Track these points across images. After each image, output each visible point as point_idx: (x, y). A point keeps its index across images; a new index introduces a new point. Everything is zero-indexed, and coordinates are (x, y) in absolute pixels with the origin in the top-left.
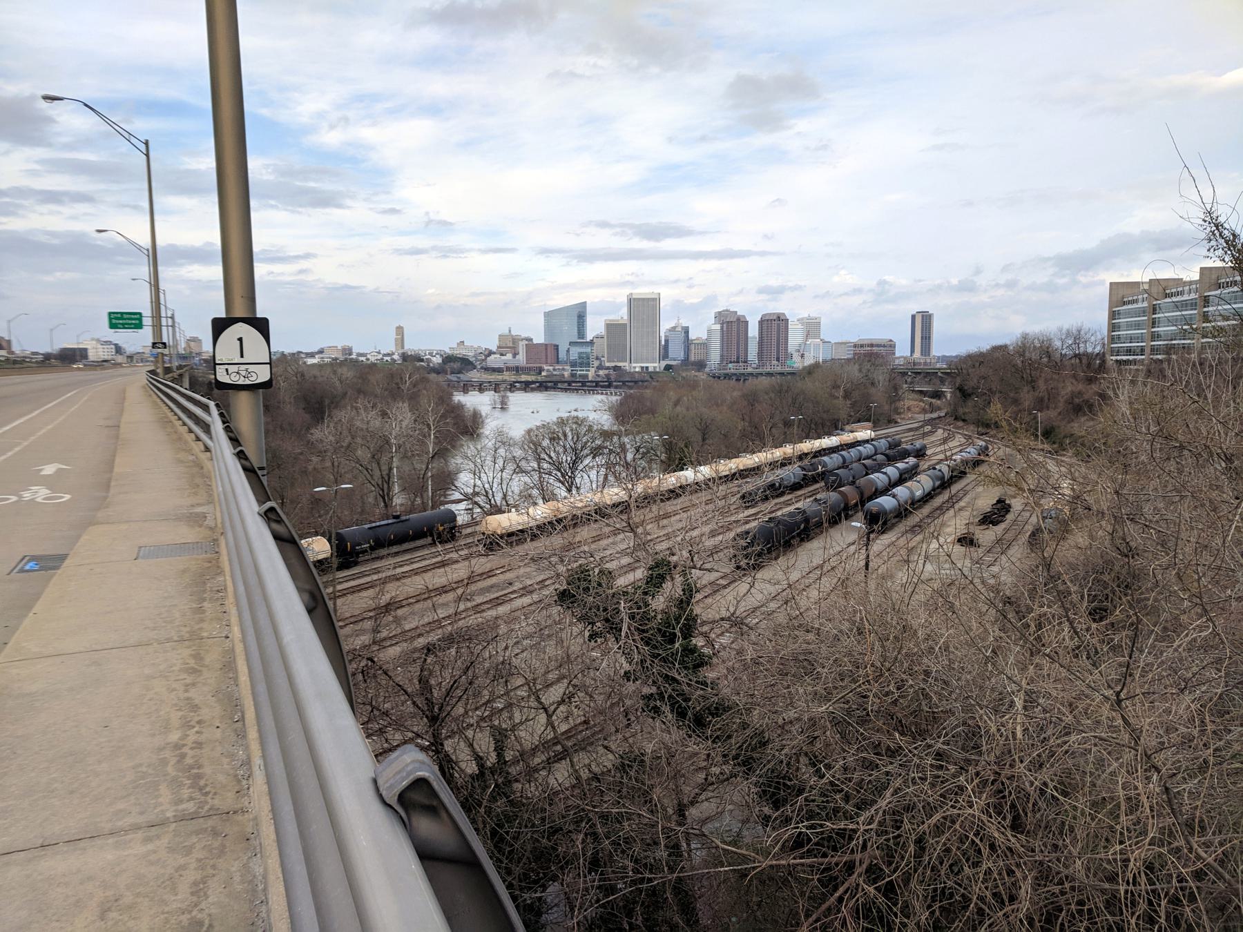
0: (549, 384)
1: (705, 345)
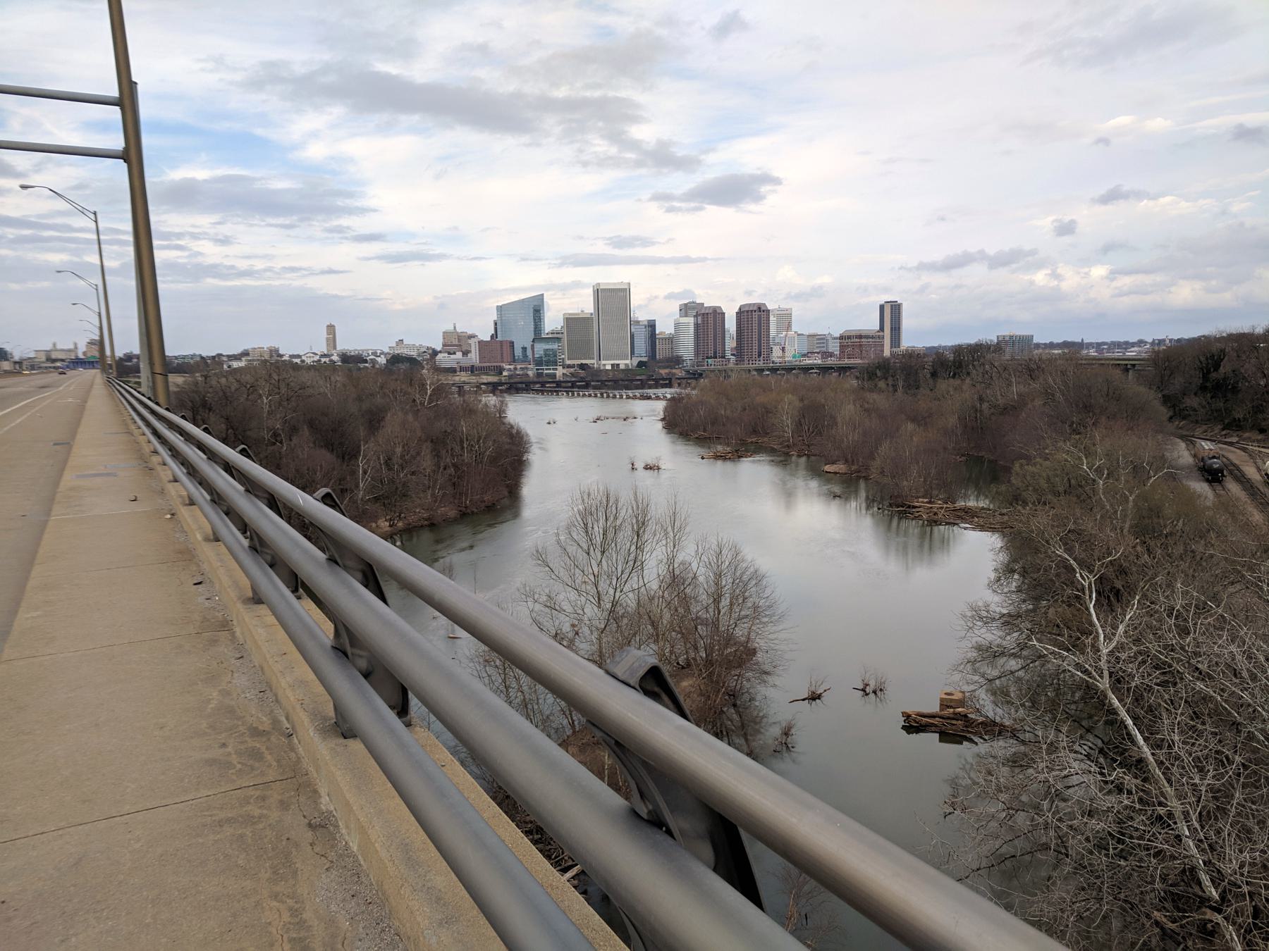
0: (520, 385)
1: (671, 340)
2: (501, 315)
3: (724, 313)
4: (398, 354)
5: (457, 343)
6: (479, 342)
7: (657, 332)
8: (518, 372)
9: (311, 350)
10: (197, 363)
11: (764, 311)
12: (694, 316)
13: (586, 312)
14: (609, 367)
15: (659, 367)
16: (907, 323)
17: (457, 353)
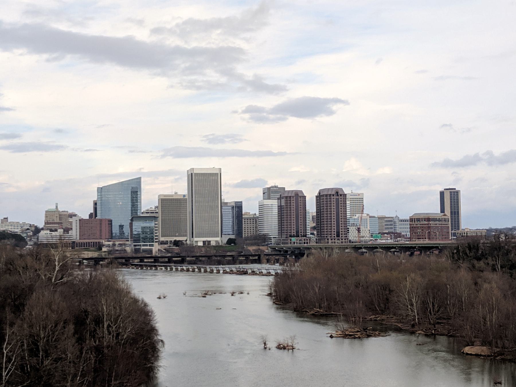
2: (101, 195)
4: (4, 231)
6: (80, 220)
7: (243, 213)
8: (117, 248)
11: (341, 195)
12: (278, 199)
13: (179, 193)
14: (201, 244)
15: (248, 245)
16: (464, 209)
17: (59, 230)
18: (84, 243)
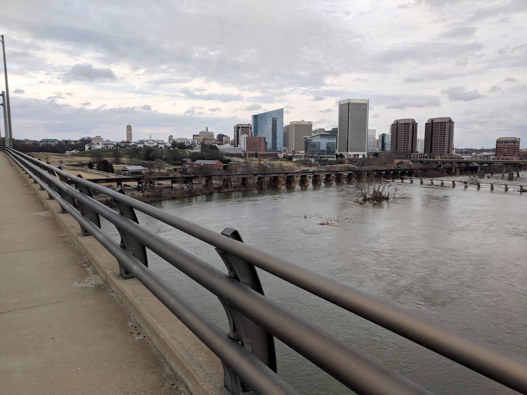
3: (417, 123)
5: (209, 138)
9: (151, 137)
10: (57, 146)
18: (269, 154)
